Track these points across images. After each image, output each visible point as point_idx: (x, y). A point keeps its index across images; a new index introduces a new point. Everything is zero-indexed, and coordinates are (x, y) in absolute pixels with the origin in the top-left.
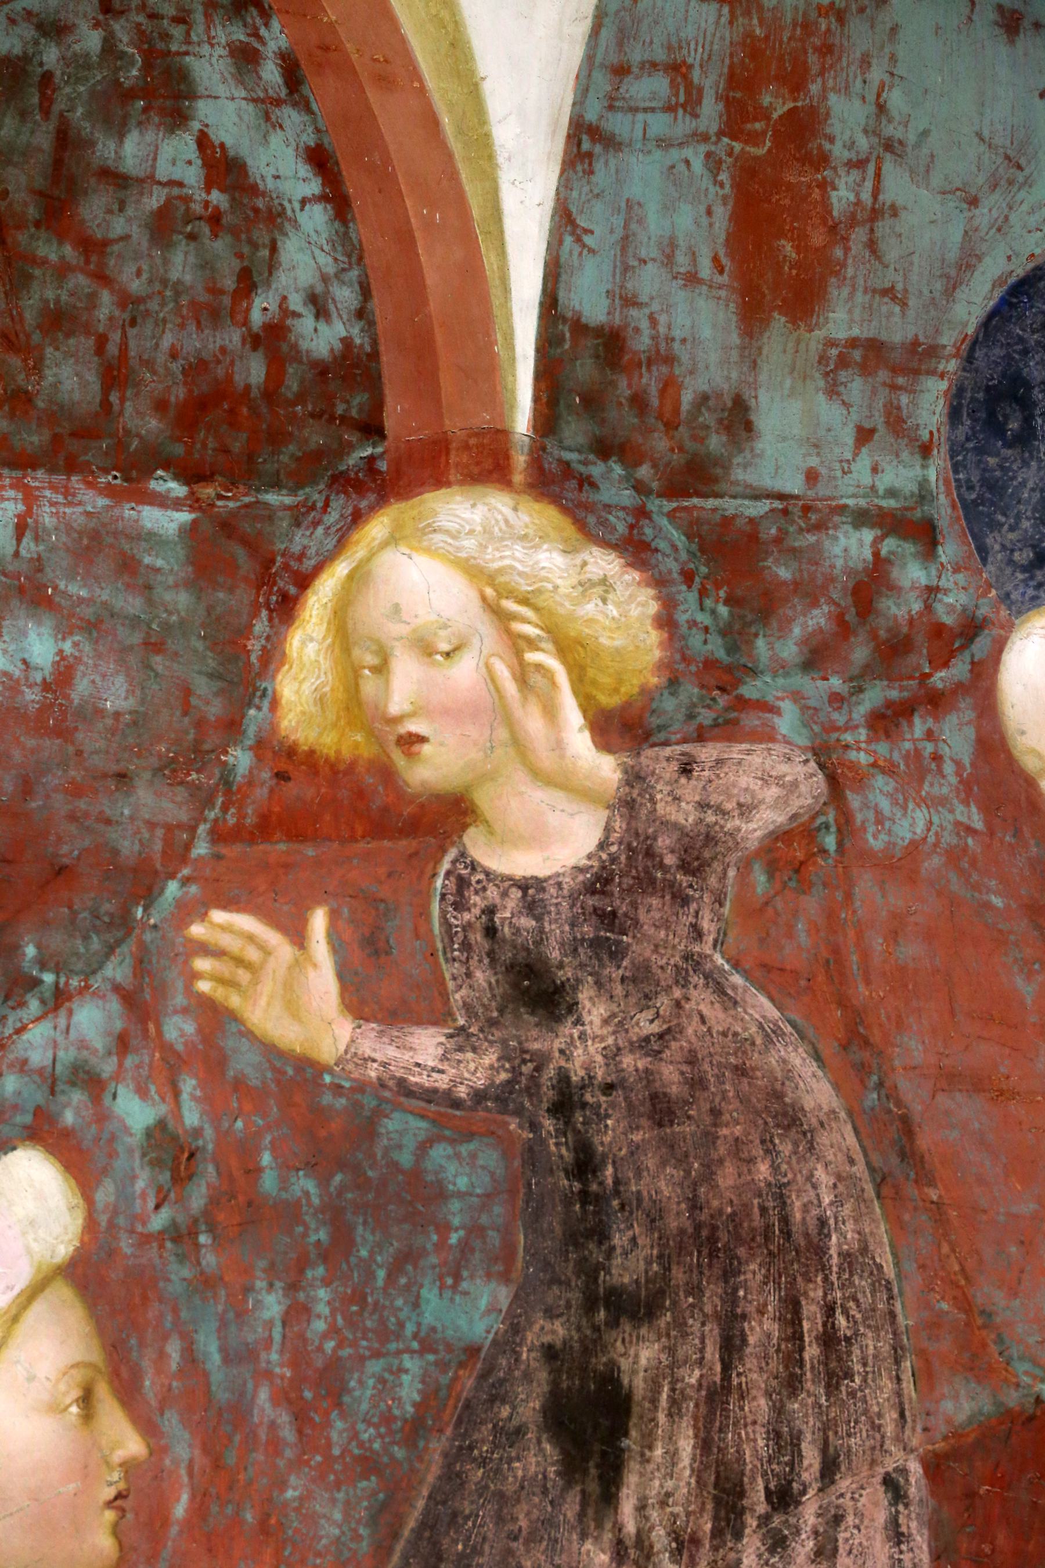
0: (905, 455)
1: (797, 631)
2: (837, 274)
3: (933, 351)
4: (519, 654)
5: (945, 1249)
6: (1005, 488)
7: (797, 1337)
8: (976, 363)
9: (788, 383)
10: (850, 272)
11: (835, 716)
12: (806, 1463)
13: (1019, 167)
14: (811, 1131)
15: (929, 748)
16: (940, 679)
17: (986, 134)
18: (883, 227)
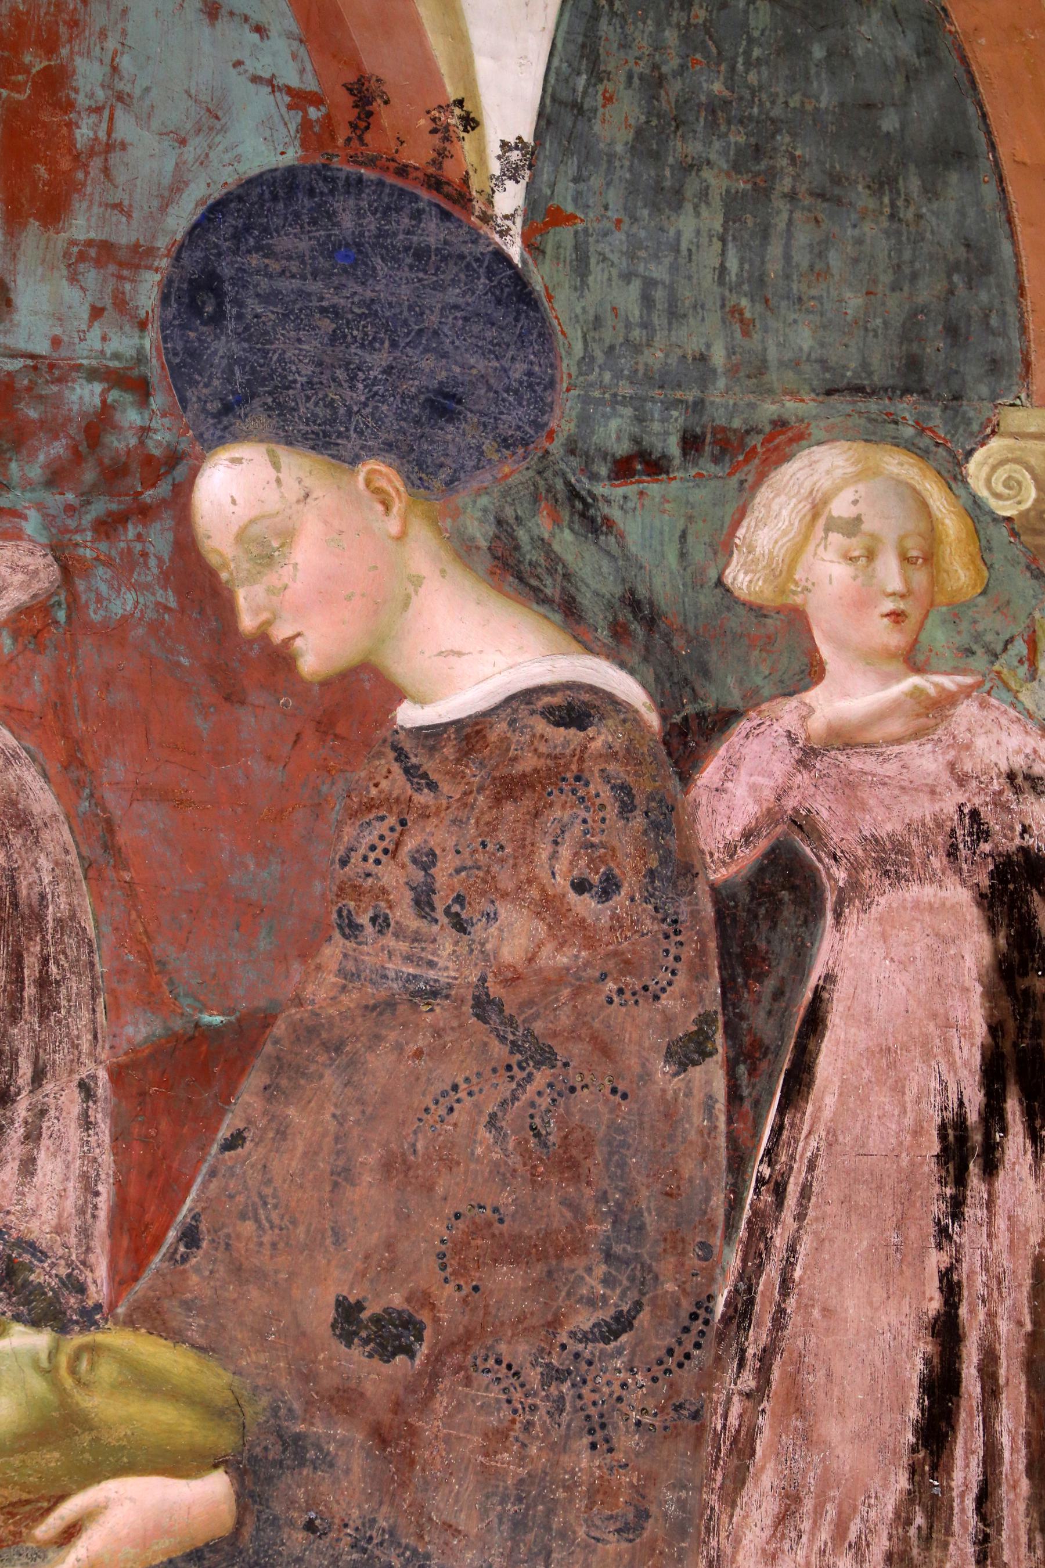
0: (127, 328)
1: (41, 458)
2: (79, 191)
3: (151, 252)
5: (134, 916)
6: (201, 355)
7: (20, 981)
8: (182, 262)
9: (40, 271)
10: (89, 190)
11: (69, 522)
12: (21, 1072)
13: (217, 118)
14: (37, 830)
15: (139, 547)
16: (149, 496)
17: (193, 92)
18: (115, 158)
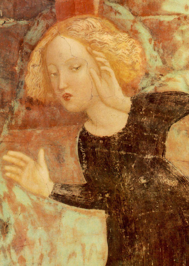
4: (99, 68)
